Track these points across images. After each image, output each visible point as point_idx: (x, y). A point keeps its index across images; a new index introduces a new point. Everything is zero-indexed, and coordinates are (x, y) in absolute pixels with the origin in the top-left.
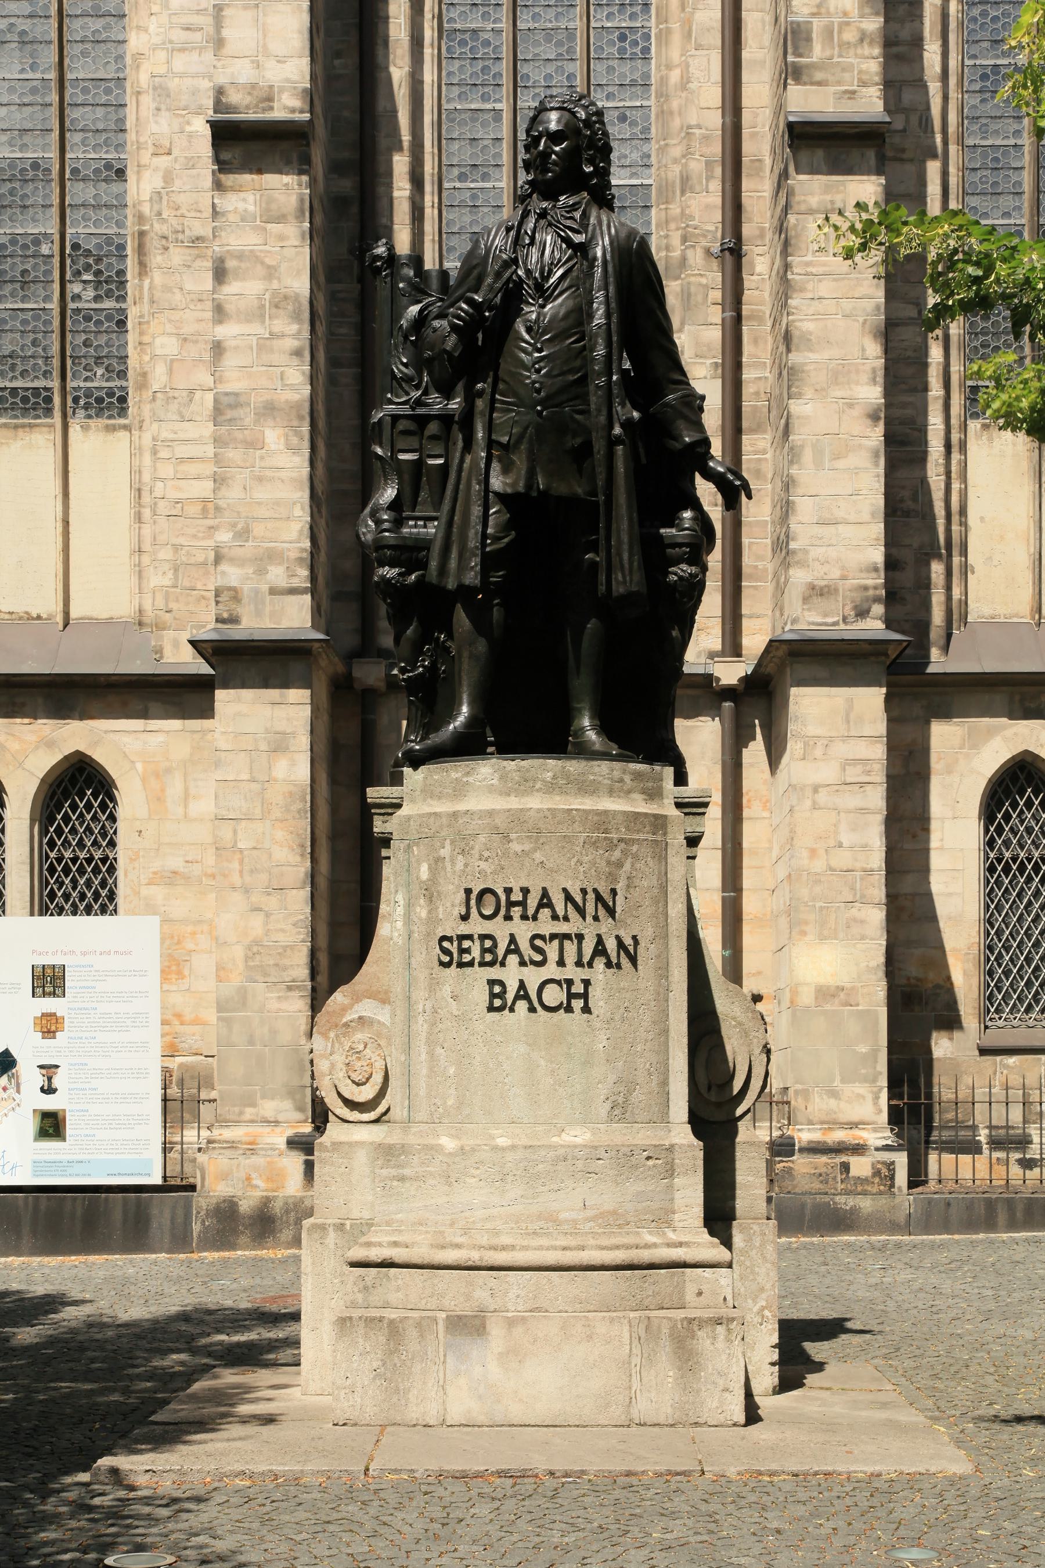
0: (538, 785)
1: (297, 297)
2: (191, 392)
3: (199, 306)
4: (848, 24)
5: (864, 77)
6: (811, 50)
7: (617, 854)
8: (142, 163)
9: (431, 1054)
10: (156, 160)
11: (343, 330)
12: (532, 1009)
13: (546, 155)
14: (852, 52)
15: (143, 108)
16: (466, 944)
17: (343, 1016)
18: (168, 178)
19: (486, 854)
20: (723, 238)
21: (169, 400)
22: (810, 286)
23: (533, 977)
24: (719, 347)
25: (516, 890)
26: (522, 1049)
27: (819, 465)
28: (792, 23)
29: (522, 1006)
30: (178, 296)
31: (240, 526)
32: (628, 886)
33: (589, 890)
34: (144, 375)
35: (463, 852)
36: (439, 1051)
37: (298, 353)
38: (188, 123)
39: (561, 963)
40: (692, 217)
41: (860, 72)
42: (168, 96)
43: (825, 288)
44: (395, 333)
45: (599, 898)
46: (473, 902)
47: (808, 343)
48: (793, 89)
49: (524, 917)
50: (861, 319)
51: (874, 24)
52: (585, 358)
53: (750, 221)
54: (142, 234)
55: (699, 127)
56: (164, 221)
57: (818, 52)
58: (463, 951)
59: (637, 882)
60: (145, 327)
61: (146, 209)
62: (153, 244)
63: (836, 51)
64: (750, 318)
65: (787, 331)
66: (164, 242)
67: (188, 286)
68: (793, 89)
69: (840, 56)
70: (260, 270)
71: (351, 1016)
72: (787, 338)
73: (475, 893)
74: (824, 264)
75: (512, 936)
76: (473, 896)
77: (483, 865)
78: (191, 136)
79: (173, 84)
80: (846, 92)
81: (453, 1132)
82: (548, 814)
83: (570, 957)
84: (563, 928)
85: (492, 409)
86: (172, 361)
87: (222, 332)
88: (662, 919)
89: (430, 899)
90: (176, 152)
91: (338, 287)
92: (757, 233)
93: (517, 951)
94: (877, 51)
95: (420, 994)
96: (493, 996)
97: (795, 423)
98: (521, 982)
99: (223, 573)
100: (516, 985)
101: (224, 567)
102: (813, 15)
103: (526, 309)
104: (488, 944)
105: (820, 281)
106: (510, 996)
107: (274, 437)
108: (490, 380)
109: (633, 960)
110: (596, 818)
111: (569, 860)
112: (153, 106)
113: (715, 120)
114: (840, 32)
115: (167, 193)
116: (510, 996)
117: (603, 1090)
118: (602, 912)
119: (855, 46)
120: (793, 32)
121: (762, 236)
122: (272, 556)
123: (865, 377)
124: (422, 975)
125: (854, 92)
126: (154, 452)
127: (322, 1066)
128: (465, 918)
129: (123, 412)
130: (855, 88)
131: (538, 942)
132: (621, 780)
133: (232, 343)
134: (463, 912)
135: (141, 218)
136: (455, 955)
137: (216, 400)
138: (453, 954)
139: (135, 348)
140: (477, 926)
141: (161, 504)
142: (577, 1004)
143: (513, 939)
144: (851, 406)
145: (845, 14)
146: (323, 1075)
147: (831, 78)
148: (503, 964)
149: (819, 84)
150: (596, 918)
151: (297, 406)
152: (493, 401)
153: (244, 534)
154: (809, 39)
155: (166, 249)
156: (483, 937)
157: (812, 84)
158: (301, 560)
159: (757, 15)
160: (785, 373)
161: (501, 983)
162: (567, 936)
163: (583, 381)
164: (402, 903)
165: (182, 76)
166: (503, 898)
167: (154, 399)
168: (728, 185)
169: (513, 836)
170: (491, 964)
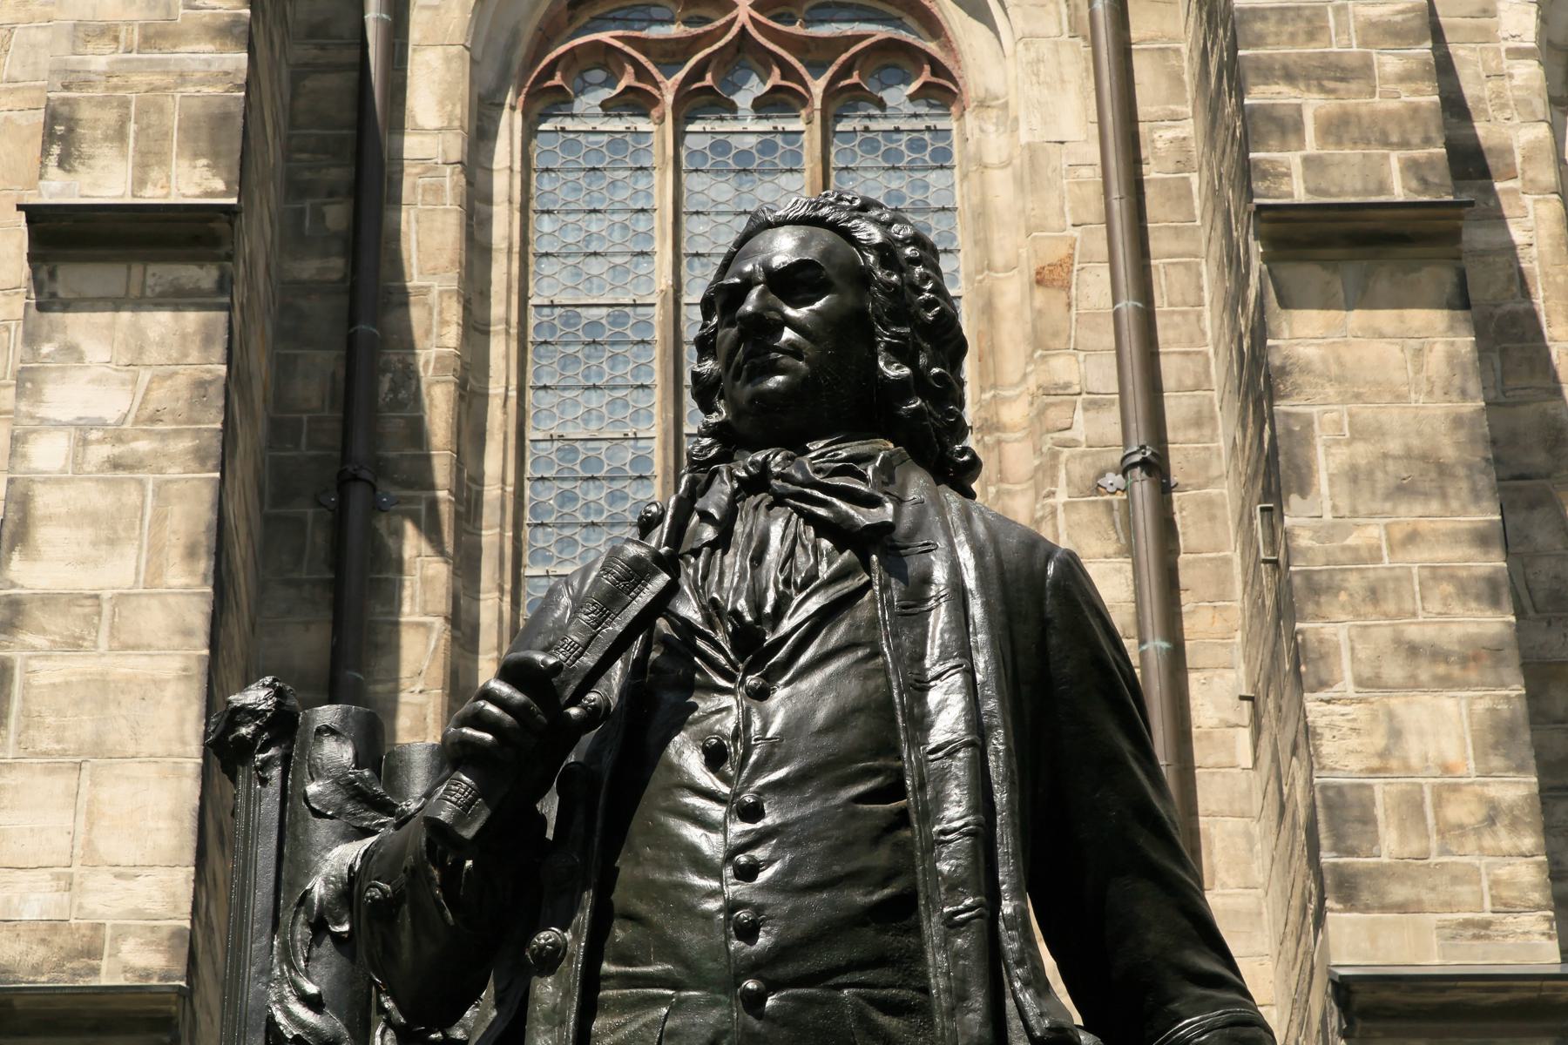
4: (1455, 788)
5: (1506, 893)
6: (1375, 841)
13: (763, 328)
14: (1471, 843)
28: (1324, 787)
41: (1495, 883)
44: (286, 917)
48: (1340, 921)
51: (1517, 788)
52: (904, 848)
57: (1390, 844)
68: (1340, 921)
69: (1444, 852)
80: (1466, 924)
85: (589, 1008)
94: (1529, 841)
102: (1373, 772)
103: (706, 704)
108: (583, 917)
114: (1438, 804)
119: (1477, 832)
120: (1330, 806)
125: (1487, 925)
130: (1488, 915)
145: (1446, 769)
147: (1426, 896)
149: (1402, 908)
152: (591, 980)
154: (1368, 820)
157: (1384, 908)
159: (1232, 823)
163: (901, 911)
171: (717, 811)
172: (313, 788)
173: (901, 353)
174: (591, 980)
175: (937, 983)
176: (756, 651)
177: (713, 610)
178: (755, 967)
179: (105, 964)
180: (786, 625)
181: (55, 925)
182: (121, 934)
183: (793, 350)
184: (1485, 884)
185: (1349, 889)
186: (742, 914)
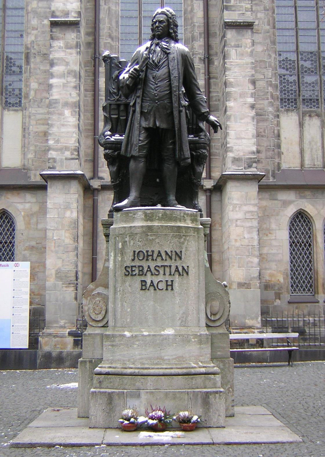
0: (157, 218)
1: (75, 71)
2: (42, 100)
3: (45, 74)
7: (182, 240)
8: (29, 32)
9: (122, 305)
10: (33, 32)
11: (89, 81)
12: (155, 290)
15: (29, 17)
16: (134, 269)
17: (92, 292)
18: (36, 36)
19: (140, 240)
20: (205, 55)
21: (35, 101)
22: (232, 69)
23: (156, 280)
24: (204, 86)
25: (150, 251)
26: (152, 303)
27: (236, 122)
29: (152, 288)
30: (38, 71)
31: (56, 139)
32: (186, 250)
33: (173, 251)
34: (27, 94)
35: (133, 239)
36: (124, 303)
37: (75, 87)
38: (43, 21)
39: (164, 274)
40: (195, 49)
41: (246, 8)
42: (37, 13)
43: (236, 70)
45: (176, 253)
46: (136, 255)
47: (231, 85)
48: (225, 12)
49: (153, 260)
50: (248, 78)
53: (213, 49)
54: (28, 53)
55: (197, 23)
56: (35, 49)
58: (132, 271)
59: (189, 249)
60: (28, 80)
61: (29, 46)
62: (31, 56)
63: (238, 2)
64: (214, 78)
65: (225, 81)
66: (35, 55)
67: (42, 68)
68: (225, 12)
69: (239, 3)
70: (64, 63)
71: (95, 292)
72: (225, 84)
73: (136, 253)
74: (236, 62)
75: (149, 267)
76: (136, 253)
77: (139, 243)
78: (44, 25)
79: (39, 10)
80: (241, 13)
81: (129, 330)
82: (160, 227)
83: (167, 273)
84: (166, 264)
86: (36, 90)
87: (53, 81)
88: (197, 260)
89: (122, 254)
90: (39, 29)
91: (87, 68)
92: (215, 53)
93: (150, 271)
95: (119, 285)
96: (142, 285)
97: (228, 109)
98: (152, 282)
99: (51, 153)
100: (150, 282)
101: (51, 152)
104: (141, 269)
105: (235, 67)
106: (148, 285)
107: (67, 112)
109: (187, 273)
110: (176, 228)
111: (167, 241)
112: (32, 16)
113: (202, 21)
115: (36, 41)
116: (148, 285)
117: (178, 316)
118: (177, 258)
121: (216, 54)
122: (67, 148)
123: (249, 96)
124: (119, 279)
125: (244, 13)
126: (30, 117)
127: (86, 308)
128: (133, 260)
129: (20, 106)
131: (157, 268)
132: (184, 216)
133: (55, 84)
134: (133, 258)
135: (27, 48)
136: (130, 272)
137: (50, 101)
138: (129, 272)
139: (25, 86)
140: (137, 263)
141: (32, 133)
142: (170, 288)
143: (149, 267)
144: (245, 104)
146: (85, 311)
147: (237, 9)
148: (145, 275)
149: (233, 11)
150: (175, 260)
151: (75, 103)
153: (57, 141)
155: (35, 57)
156: (139, 266)
157: (231, 11)
158: (75, 150)
160: (225, 94)
161: (145, 281)
162: (167, 266)
164: (113, 255)
165: (42, 8)
166: (146, 254)
167: (30, 101)
168: (206, 39)
169: (149, 234)
170: (142, 275)
171: (154, 84)
172: (113, 65)
173: (172, 29)
174: (142, 100)
175: (173, 101)
176: (157, 66)
177: (153, 61)
178: (157, 100)
179: (70, 16)
180: (160, 64)
181: (63, 11)
182: (72, 11)
183: (161, 29)
184: (244, 8)
185: (227, 8)
186: (156, 95)
